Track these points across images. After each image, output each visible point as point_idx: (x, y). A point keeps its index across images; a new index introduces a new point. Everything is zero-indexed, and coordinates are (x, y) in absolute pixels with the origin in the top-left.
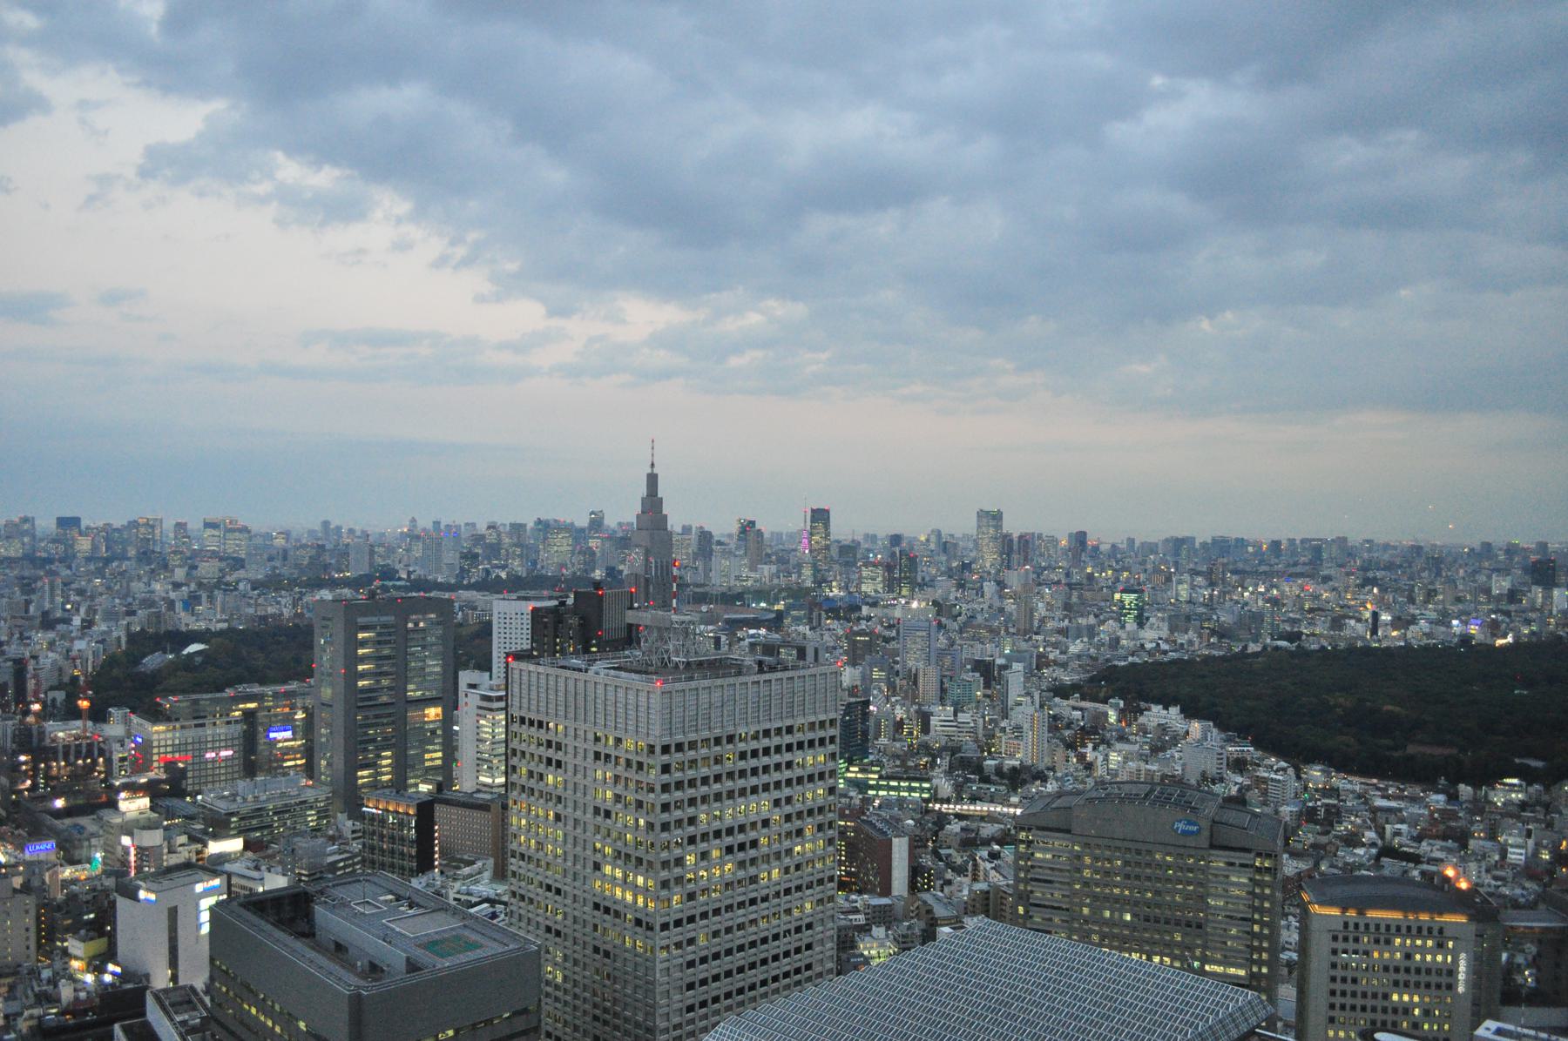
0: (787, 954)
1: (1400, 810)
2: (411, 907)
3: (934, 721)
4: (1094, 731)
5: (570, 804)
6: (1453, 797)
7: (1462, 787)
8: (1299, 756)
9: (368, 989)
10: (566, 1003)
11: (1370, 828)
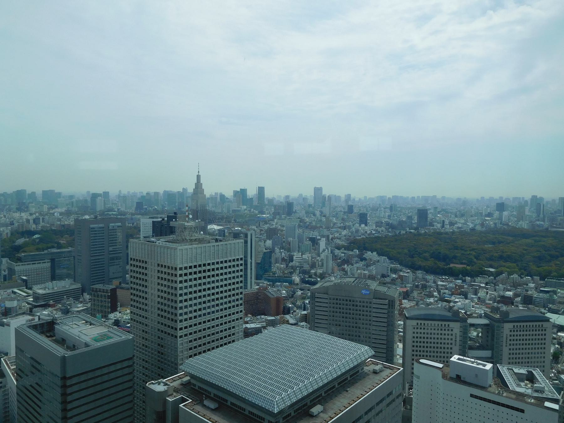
0: (225, 337)
1: (446, 285)
2: (91, 325)
3: (294, 258)
4: (347, 261)
5: (150, 288)
6: (464, 281)
7: (467, 277)
8: (414, 268)
9: (69, 353)
10: (149, 356)
11: (435, 292)
